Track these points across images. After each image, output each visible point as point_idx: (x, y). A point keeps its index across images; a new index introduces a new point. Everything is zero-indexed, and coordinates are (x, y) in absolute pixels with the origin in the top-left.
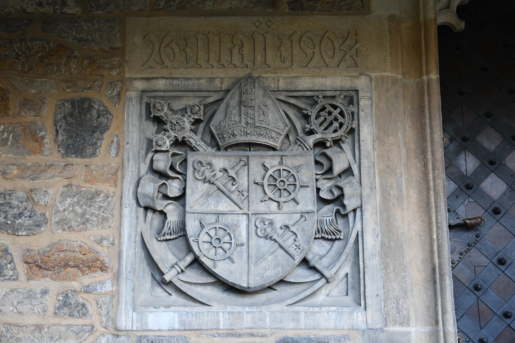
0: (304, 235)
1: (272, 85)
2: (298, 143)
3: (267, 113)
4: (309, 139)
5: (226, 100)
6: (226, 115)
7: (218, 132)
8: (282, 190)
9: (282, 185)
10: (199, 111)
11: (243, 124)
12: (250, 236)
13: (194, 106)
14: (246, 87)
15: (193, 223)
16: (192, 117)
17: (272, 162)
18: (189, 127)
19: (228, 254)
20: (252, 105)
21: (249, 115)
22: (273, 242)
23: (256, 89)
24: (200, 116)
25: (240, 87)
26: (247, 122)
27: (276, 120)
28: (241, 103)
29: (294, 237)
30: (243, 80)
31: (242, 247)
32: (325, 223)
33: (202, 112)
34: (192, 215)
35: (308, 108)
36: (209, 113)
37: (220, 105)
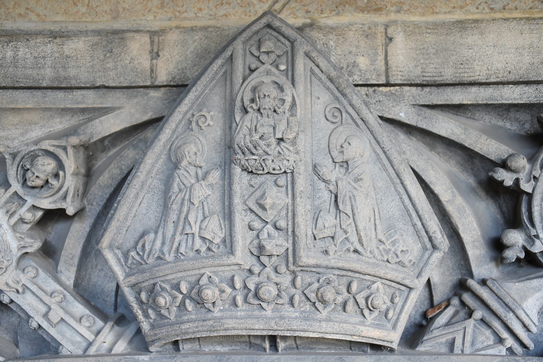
1: (363, 62)
2: (478, 314)
3: (353, 198)
4: (524, 298)
5: (166, 133)
6: (165, 207)
7: (133, 280)
10: (56, 176)
11: (242, 256)
13: (33, 157)
14: (254, 79)
16: (30, 201)
18: (14, 244)
20: (285, 165)
21: (270, 216)
23: (300, 87)
24: (65, 198)
25: (228, 76)
26: (261, 248)
27: (390, 228)
28: (230, 152)
30: (238, 45)
33: (71, 182)
35: (521, 162)
36: (105, 180)
37: (148, 145)
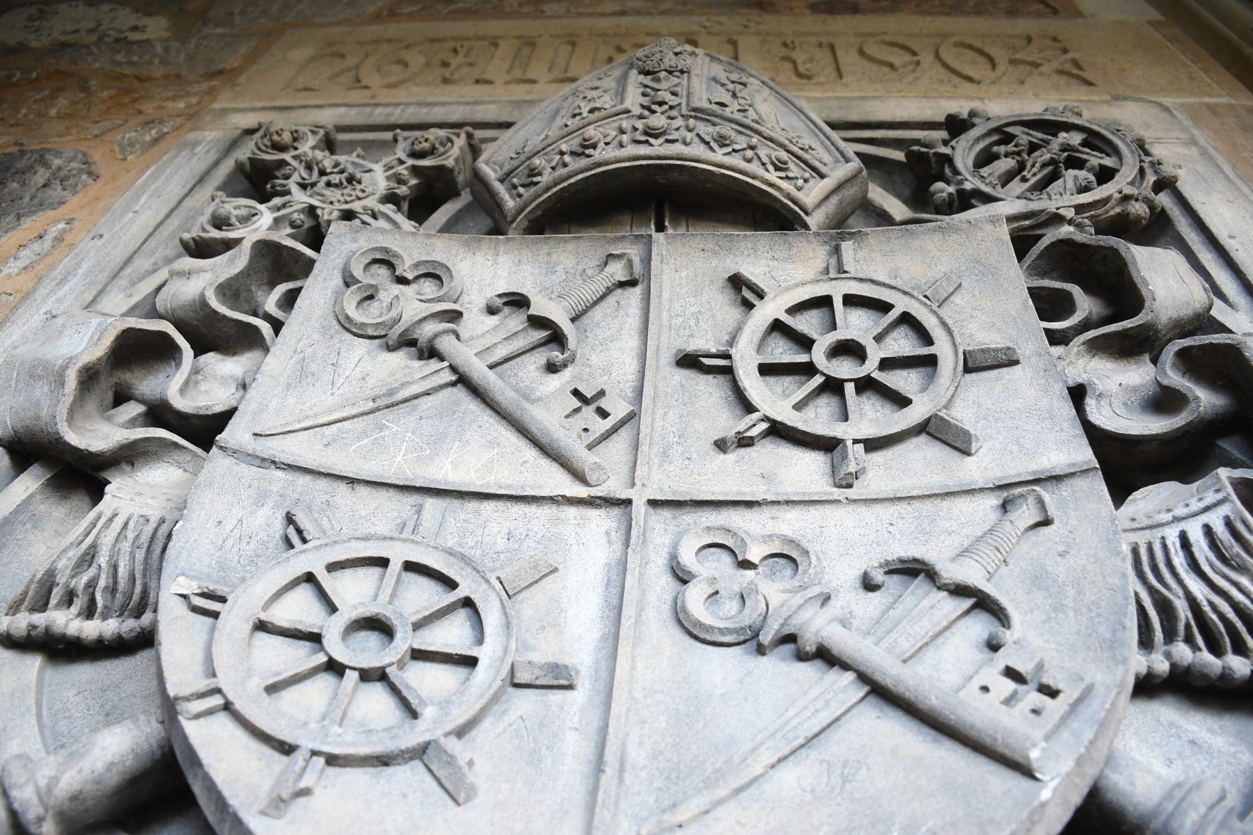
0: (1059, 608)
8: (850, 388)
9: (845, 381)
12: (626, 623)
15: (237, 512)
17: (786, 271)
19: (421, 724)
22: (809, 671)
29: (979, 627)
31: (556, 697)
32: (1179, 560)
34: (249, 472)
